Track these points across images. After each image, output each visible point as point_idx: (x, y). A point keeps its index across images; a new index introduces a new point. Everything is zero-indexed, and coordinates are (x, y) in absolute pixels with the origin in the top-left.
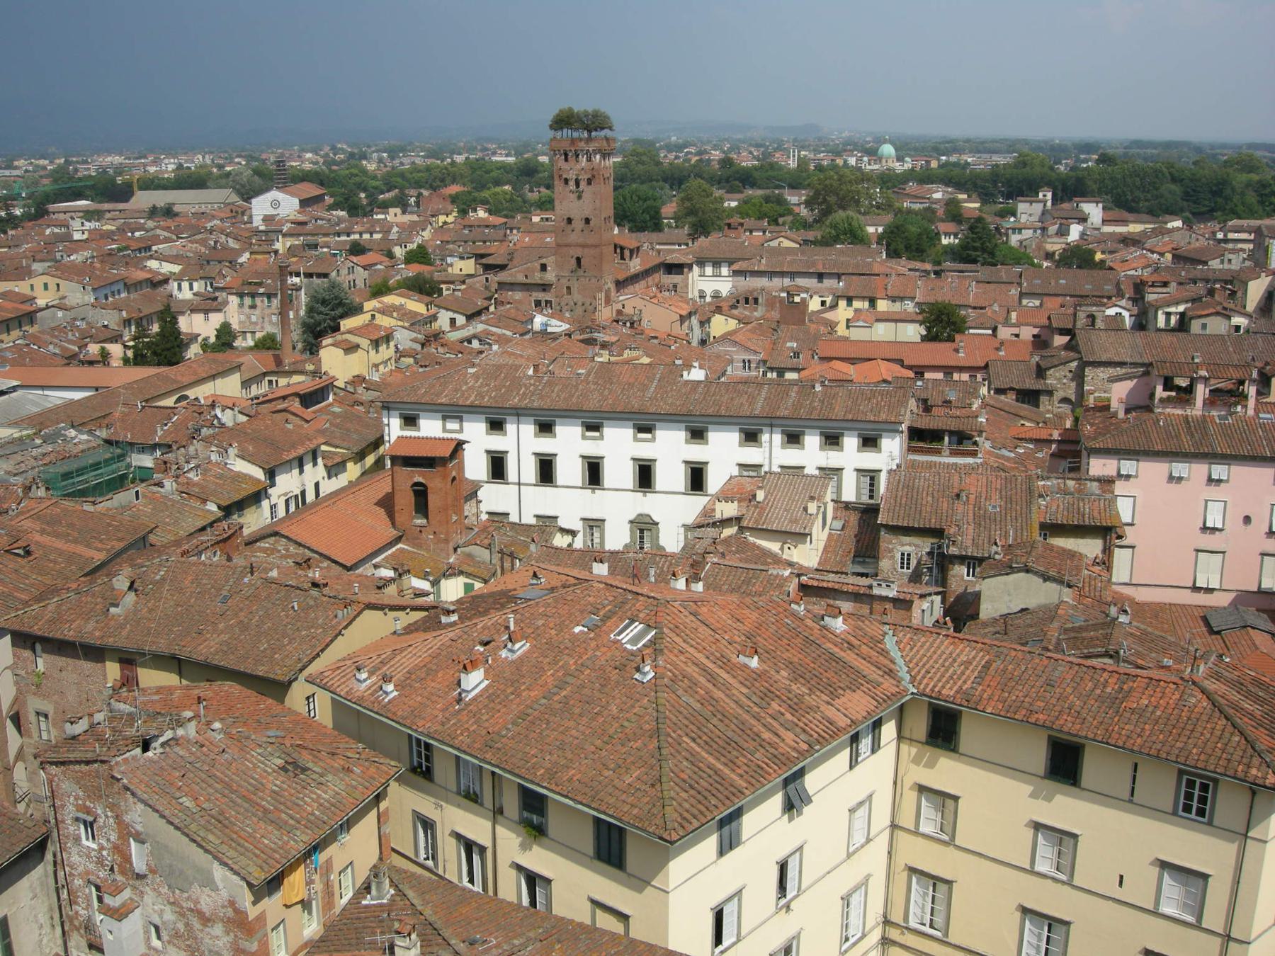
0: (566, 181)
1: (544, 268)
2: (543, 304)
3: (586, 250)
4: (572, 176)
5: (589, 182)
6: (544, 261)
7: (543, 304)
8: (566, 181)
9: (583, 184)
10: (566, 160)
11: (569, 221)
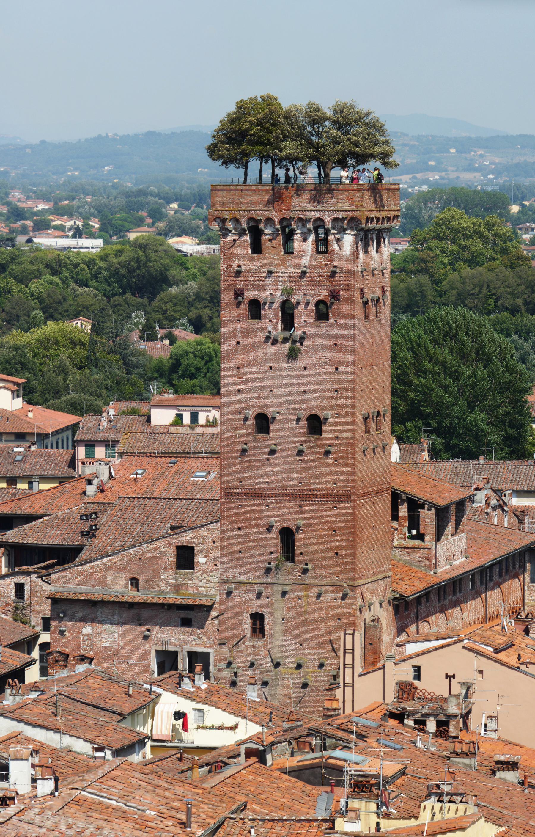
0: (256, 309)
1: (186, 558)
2: (183, 663)
3: (309, 509)
4: (272, 293)
5: (322, 313)
6: (186, 538)
7: (183, 663)
8: (256, 309)
9: (303, 317)
10: (257, 247)
11: (263, 423)
